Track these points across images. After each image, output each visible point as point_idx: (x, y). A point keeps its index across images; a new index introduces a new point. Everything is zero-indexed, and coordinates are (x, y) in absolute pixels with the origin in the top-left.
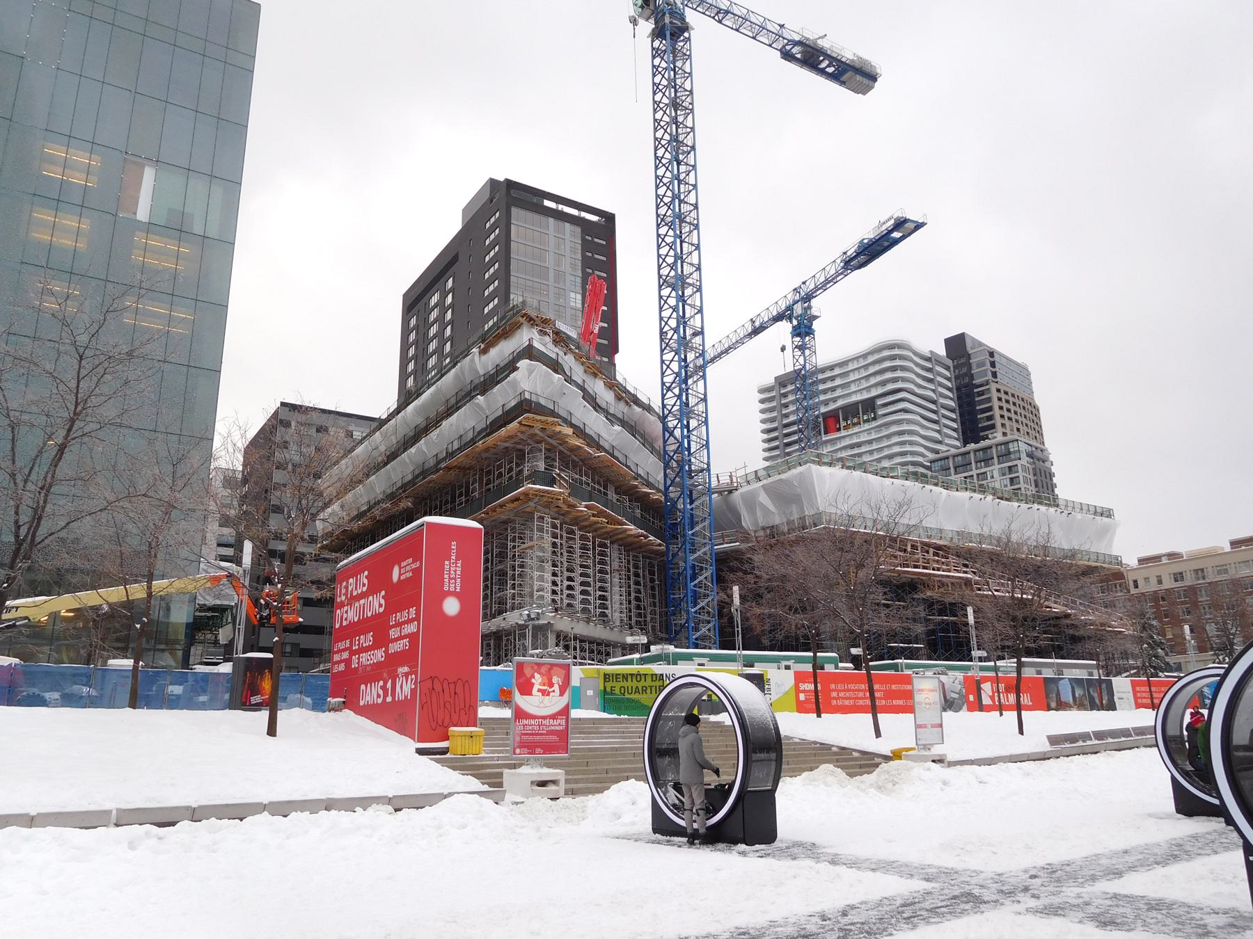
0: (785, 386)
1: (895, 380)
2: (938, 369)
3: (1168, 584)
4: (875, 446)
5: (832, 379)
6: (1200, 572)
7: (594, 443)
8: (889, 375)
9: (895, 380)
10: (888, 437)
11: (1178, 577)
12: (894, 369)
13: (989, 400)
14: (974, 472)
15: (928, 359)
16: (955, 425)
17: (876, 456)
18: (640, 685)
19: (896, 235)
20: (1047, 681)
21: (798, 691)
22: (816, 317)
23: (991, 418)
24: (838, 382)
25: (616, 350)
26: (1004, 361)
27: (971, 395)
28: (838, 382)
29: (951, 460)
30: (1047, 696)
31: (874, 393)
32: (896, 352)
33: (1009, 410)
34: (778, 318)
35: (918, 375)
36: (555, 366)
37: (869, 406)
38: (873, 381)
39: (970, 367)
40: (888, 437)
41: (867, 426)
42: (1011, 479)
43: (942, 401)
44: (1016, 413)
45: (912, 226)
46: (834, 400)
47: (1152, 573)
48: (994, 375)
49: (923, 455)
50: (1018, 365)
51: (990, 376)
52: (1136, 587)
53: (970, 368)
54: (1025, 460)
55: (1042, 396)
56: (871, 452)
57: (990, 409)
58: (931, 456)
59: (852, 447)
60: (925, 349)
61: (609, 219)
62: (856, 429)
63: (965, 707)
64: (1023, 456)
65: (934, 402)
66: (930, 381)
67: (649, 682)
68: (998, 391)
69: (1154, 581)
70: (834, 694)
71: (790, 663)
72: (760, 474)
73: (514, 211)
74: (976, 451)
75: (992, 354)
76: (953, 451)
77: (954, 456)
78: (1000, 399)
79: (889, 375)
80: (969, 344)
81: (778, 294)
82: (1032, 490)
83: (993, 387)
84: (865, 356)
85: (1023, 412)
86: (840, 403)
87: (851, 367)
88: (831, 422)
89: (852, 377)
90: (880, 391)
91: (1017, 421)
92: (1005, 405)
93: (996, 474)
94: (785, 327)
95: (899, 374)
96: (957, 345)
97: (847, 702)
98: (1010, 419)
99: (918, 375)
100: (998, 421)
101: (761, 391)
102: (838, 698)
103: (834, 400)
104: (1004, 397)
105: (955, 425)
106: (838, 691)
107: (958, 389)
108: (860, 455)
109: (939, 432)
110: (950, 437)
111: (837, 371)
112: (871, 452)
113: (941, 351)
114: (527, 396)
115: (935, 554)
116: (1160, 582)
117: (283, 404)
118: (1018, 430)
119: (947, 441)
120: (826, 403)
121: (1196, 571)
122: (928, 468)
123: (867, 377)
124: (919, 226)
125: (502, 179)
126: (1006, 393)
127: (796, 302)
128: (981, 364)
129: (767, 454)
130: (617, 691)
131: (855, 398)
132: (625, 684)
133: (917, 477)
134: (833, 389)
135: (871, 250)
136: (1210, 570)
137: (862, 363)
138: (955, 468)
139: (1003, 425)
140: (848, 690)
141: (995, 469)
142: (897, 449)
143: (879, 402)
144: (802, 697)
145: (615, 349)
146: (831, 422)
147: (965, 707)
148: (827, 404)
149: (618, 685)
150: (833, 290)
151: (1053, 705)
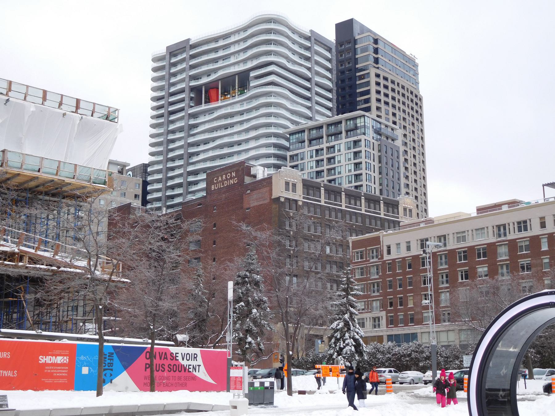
0: (175, 55)
1: (268, 53)
2: (317, 48)
3: (416, 251)
4: (245, 117)
5: (216, 50)
6: (442, 238)
9: (268, 53)
10: (257, 108)
12: (268, 42)
13: (368, 84)
14: (324, 145)
15: (308, 39)
16: (330, 104)
24: (221, 53)
26: (388, 50)
27: (353, 79)
28: (221, 53)
31: (250, 65)
32: (272, 26)
33: (386, 95)
35: (294, 52)
39: (355, 51)
40: (257, 108)
43: (318, 79)
46: (215, 71)
48: (376, 61)
50: (403, 54)
51: (371, 61)
52: (389, 252)
53: (355, 54)
54: (370, 135)
56: (241, 123)
57: (368, 92)
65: (308, 80)
66: (308, 59)
68: (378, 76)
69: (403, 247)
77: (310, 129)
78: (378, 84)
80: (356, 30)
83: (373, 72)
84: (245, 29)
85: (402, 99)
86: (220, 73)
87: (233, 39)
89: (233, 49)
90: (255, 63)
91: (394, 106)
92: (383, 90)
93: (342, 147)
95: (272, 48)
96: (345, 29)
98: (386, 103)
99: (294, 52)
101: (155, 60)
103: (215, 71)
105: (330, 104)
109: (309, 108)
111: (221, 43)
112: (241, 123)
113: (331, 36)
116: (409, 248)
118: (394, 115)
120: (208, 73)
122: (288, 140)
126: (386, 79)
128: (365, 49)
129: (154, 121)
134: (215, 60)
137: (243, 35)
139: (378, 109)
141: (342, 143)
143: (252, 74)
146: (213, 93)
148: (209, 75)
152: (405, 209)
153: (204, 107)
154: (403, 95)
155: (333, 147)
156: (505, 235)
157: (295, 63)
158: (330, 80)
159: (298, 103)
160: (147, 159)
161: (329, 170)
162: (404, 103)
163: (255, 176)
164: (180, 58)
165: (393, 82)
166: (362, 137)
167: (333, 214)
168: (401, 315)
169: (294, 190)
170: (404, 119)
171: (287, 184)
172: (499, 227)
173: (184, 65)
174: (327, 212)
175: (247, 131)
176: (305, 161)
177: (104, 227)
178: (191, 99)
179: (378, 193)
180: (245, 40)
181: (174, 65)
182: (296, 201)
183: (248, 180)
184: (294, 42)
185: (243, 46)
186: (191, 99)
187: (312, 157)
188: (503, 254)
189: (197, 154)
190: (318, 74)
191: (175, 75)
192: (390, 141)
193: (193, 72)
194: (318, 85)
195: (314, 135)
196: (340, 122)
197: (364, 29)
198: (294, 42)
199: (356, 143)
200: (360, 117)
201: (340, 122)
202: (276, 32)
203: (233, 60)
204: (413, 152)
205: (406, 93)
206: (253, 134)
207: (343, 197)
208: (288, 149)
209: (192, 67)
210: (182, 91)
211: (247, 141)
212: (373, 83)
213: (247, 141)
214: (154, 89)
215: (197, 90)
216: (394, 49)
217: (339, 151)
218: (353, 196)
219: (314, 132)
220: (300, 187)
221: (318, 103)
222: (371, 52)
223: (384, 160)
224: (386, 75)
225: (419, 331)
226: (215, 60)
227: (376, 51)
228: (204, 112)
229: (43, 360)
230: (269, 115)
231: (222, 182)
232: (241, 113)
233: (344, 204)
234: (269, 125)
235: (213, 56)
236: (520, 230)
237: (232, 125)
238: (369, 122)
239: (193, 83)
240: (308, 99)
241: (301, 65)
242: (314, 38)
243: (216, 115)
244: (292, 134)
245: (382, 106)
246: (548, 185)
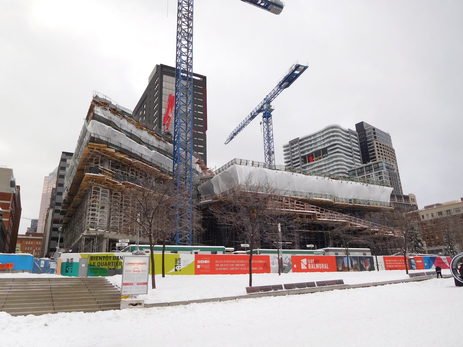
1: (334, 140)
2: (352, 135)
3: (436, 216)
4: (327, 166)
5: (311, 141)
6: (448, 211)
7: (140, 158)
8: (332, 139)
9: (334, 140)
10: (332, 162)
11: (440, 213)
12: (333, 136)
13: (373, 147)
14: (365, 175)
15: (348, 132)
16: (359, 157)
17: (328, 170)
18: (107, 262)
19: (297, 72)
20: (337, 258)
21: (196, 264)
22: (272, 110)
23: (374, 154)
24: (313, 142)
25: (206, 129)
26: (379, 132)
27: (366, 146)
28: (313, 142)
29: (356, 171)
30: (337, 265)
31: (326, 146)
32: (334, 129)
33: (381, 151)
34: (259, 111)
35: (344, 138)
36: (108, 122)
37: (325, 151)
38: (326, 141)
40: (332, 162)
41: (325, 159)
42: (380, 177)
43: (354, 148)
45: (303, 68)
46: (312, 149)
47: (430, 212)
48: (375, 137)
49: (346, 169)
50: (385, 133)
51: (373, 138)
54: (385, 170)
55: (395, 145)
56: (326, 169)
57: (374, 151)
58: (349, 169)
59: (318, 167)
60: (346, 127)
61: (204, 78)
62: (321, 160)
63: (291, 270)
64: (385, 168)
65: (350, 149)
66: (349, 140)
67: (112, 260)
68: (377, 143)
69: (430, 216)
70: (218, 265)
71: (198, 251)
72: (220, 170)
73: (164, 76)
74: (366, 167)
75: (374, 129)
76: (357, 167)
77: (357, 169)
78: (377, 147)
79: (332, 139)
81: (258, 102)
82: (389, 181)
83: (375, 142)
84: (322, 132)
85: (387, 152)
86: (314, 150)
87: (317, 136)
88: (311, 158)
89: (318, 140)
90: (329, 145)
91: (385, 155)
93: (374, 175)
94: (261, 114)
95: (335, 138)
96: (360, 126)
97: (224, 269)
98: (382, 154)
99: (344, 138)
100: (377, 155)
101: (284, 147)
102: (220, 267)
103: (312, 149)
104: (379, 146)
105: (359, 157)
106: (220, 264)
107: (361, 144)
108: (322, 170)
109: (352, 160)
110: (358, 162)
111: (312, 138)
112: (326, 169)
113: (354, 129)
114: (92, 135)
115: (297, 203)
117: (63, 153)
118: (385, 158)
119: (356, 164)
120: (308, 150)
121: (447, 211)
123: (324, 140)
124: (305, 68)
125: (159, 64)
126: (380, 144)
127: (264, 104)
130: (96, 265)
131: (319, 148)
132: (100, 261)
133: (345, 178)
134: (311, 145)
135: (290, 79)
136: (453, 210)
137: (322, 134)
138: (358, 174)
139: (379, 157)
140: (225, 263)
141: (373, 173)
142: (335, 167)
143: (328, 149)
144: (198, 267)
145: (205, 128)
146: (311, 158)
147: (291, 270)
149: (97, 262)
150: (278, 98)
151: (340, 269)
152: (412, 199)
153: (308, 164)
157: (344, 143)
159: (348, 159)
164: (295, 145)
165: (383, 145)
168: (433, 242)
185: (322, 138)
191: (293, 152)
193: (301, 151)
194: (355, 150)
195: (360, 172)
196: (371, 165)
202: (336, 132)
203: (318, 144)
205: (384, 147)
209: (301, 148)
210: (298, 158)
212: (375, 147)
214: (285, 159)
215: (304, 157)
216: (381, 132)
219: (360, 170)
221: (355, 158)
222: (373, 134)
223: (392, 179)
224: (380, 143)
225: (443, 248)
226: (311, 145)
228: (308, 166)
234: (338, 169)
235: (309, 143)
239: (302, 155)
240: (351, 156)
242: (350, 132)
245: (380, 155)
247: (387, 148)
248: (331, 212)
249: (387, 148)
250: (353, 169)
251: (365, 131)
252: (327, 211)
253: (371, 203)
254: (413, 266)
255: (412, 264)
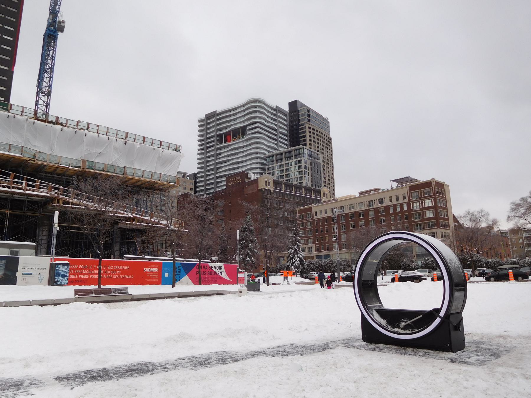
0: (209, 119)
3: (329, 214)
4: (244, 149)
5: (230, 116)
6: (342, 208)
10: (250, 145)
13: (305, 132)
14: (284, 163)
15: (275, 110)
16: (286, 143)
24: (232, 118)
28: (232, 118)
31: (246, 123)
33: (314, 138)
35: (268, 117)
40: (250, 145)
44: (318, 139)
46: (229, 126)
48: (309, 121)
50: (322, 117)
51: (306, 121)
52: (316, 215)
53: (298, 117)
54: (306, 158)
55: (334, 133)
56: (243, 152)
57: (305, 136)
60: (274, 104)
64: (307, 156)
65: (276, 130)
66: (275, 120)
68: (310, 128)
69: (323, 212)
75: (309, 111)
77: (277, 155)
78: (310, 132)
83: (307, 126)
86: (232, 127)
87: (238, 111)
89: (238, 116)
90: (249, 122)
91: (318, 143)
92: (312, 135)
93: (293, 164)
95: (257, 115)
96: (294, 105)
98: (314, 142)
99: (268, 117)
101: (199, 121)
103: (229, 126)
104: (312, 131)
105: (286, 143)
109: (276, 144)
111: (232, 113)
112: (243, 152)
113: (286, 108)
116: (326, 213)
118: (318, 147)
120: (226, 128)
122: (266, 160)
123: (244, 116)
126: (314, 129)
128: (303, 115)
129: (199, 152)
134: (229, 121)
136: (346, 207)
137: (243, 109)
139: (310, 144)
141: (292, 162)
146: (228, 137)
148: (226, 129)
152: (324, 194)
153: (224, 144)
154: (322, 137)
155: (288, 163)
156: (373, 205)
158: (286, 130)
159: (270, 142)
160: (196, 171)
161: (286, 175)
162: (323, 142)
163: (250, 178)
164: (212, 120)
165: (317, 131)
166: (303, 159)
167: (289, 196)
168: (322, 246)
169: (269, 185)
170: (323, 149)
171: (266, 182)
172: (369, 202)
173: (214, 124)
174: (286, 196)
175: (246, 156)
176: (275, 170)
177: (175, 204)
178: (218, 140)
179: (310, 186)
180: (244, 111)
181: (209, 123)
182: (270, 190)
183: (246, 180)
184: (268, 112)
185: (243, 114)
186: (218, 140)
187: (278, 168)
188: (372, 215)
189: (221, 168)
190: (280, 127)
191: (209, 129)
192: (316, 160)
196: (292, 151)
197: (302, 105)
198: (268, 112)
199: (300, 161)
200: (301, 148)
201: (292, 151)
203: (238, 121)
204: (327, 166)
205: (323, 136)
206: (248, 158)
207: (294, 188)
208: (266, 165)
209: (218, 125)
210: (213, 137)
211: (246, 161)
212: (307, 132)
213: (246, 161)
214: (199, 136)
215: (220, 136)
216: (318, 114)
217: (291, 165)
218: (298, 188)
220: (272, 184)
221: (280, 142)
222: (306, 116)
223: (313, 170)
224: (314, 128)
225: (331, 253)
226: (229, 121)
227: (309, 116)
229: (146, 270)
230: (256, 148)
231: (234, 181)
232: (243, 147)
233: (294, 191)
234: (256, 153)
235: (228, 119)
236: (380, 203)
237: (238, 153)
238: (306, 151)
240: (276, 140)
241: (272, 123)
242: (278, 110)
243: (230, 148)
244: (268, 157)
245: (312, 143)
246: (393, 181)
247: (321, 135)
248: (16, 177)
249: (321, 135)
250: (272, 154)
251: (298, 111)
252: (9, 175)
253: (128, 170)
254: (59, 278)
255: (59, 275)
